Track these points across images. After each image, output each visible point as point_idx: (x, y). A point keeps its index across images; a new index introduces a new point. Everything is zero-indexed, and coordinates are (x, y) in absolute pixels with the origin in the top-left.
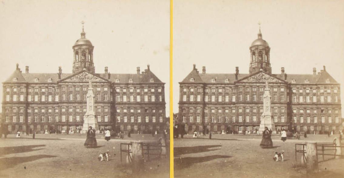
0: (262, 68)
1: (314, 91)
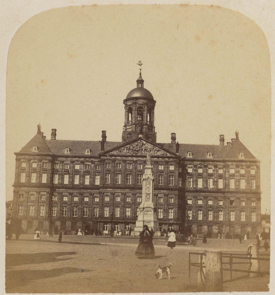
0: (141, 133)
1: (221, 172)
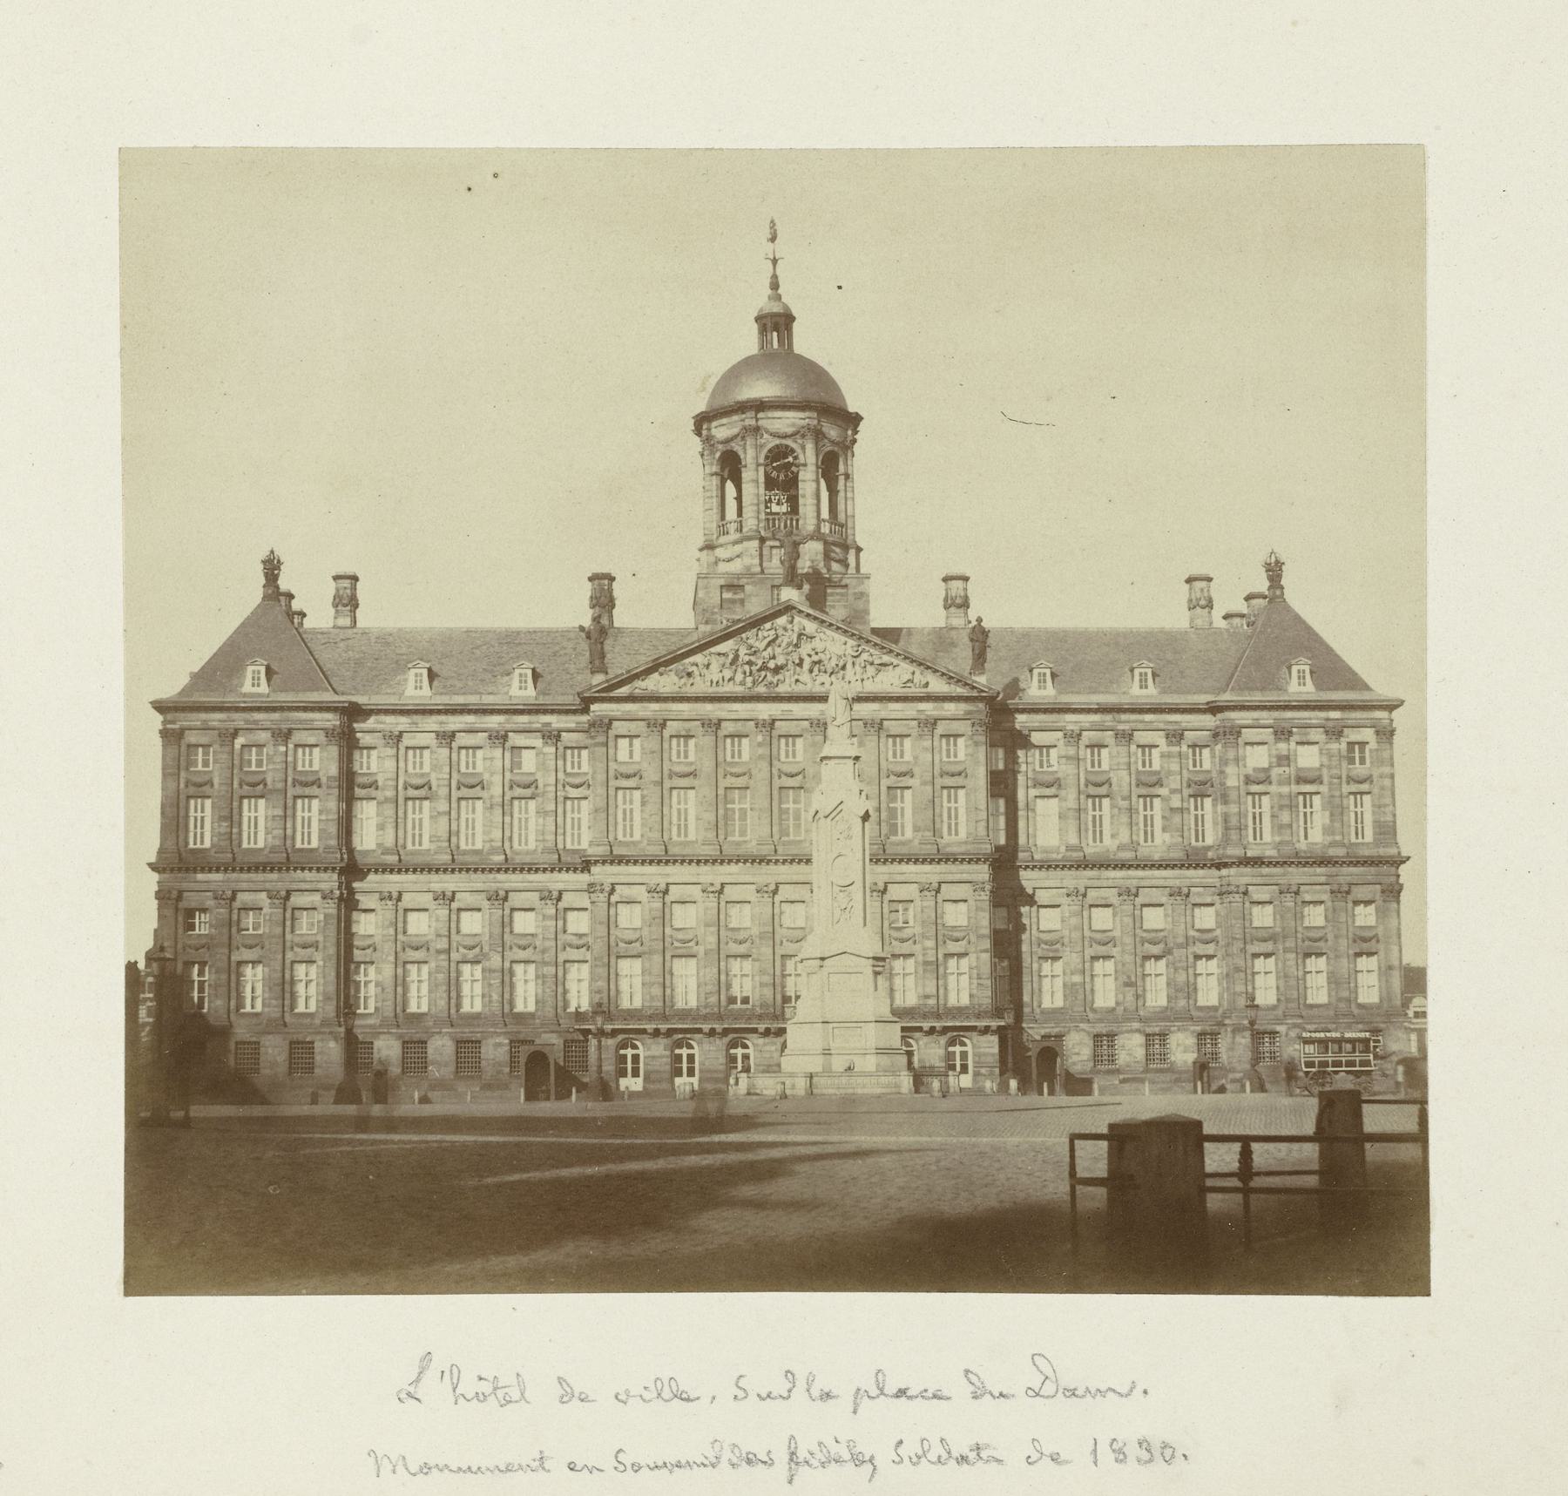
0: (792, 578)
